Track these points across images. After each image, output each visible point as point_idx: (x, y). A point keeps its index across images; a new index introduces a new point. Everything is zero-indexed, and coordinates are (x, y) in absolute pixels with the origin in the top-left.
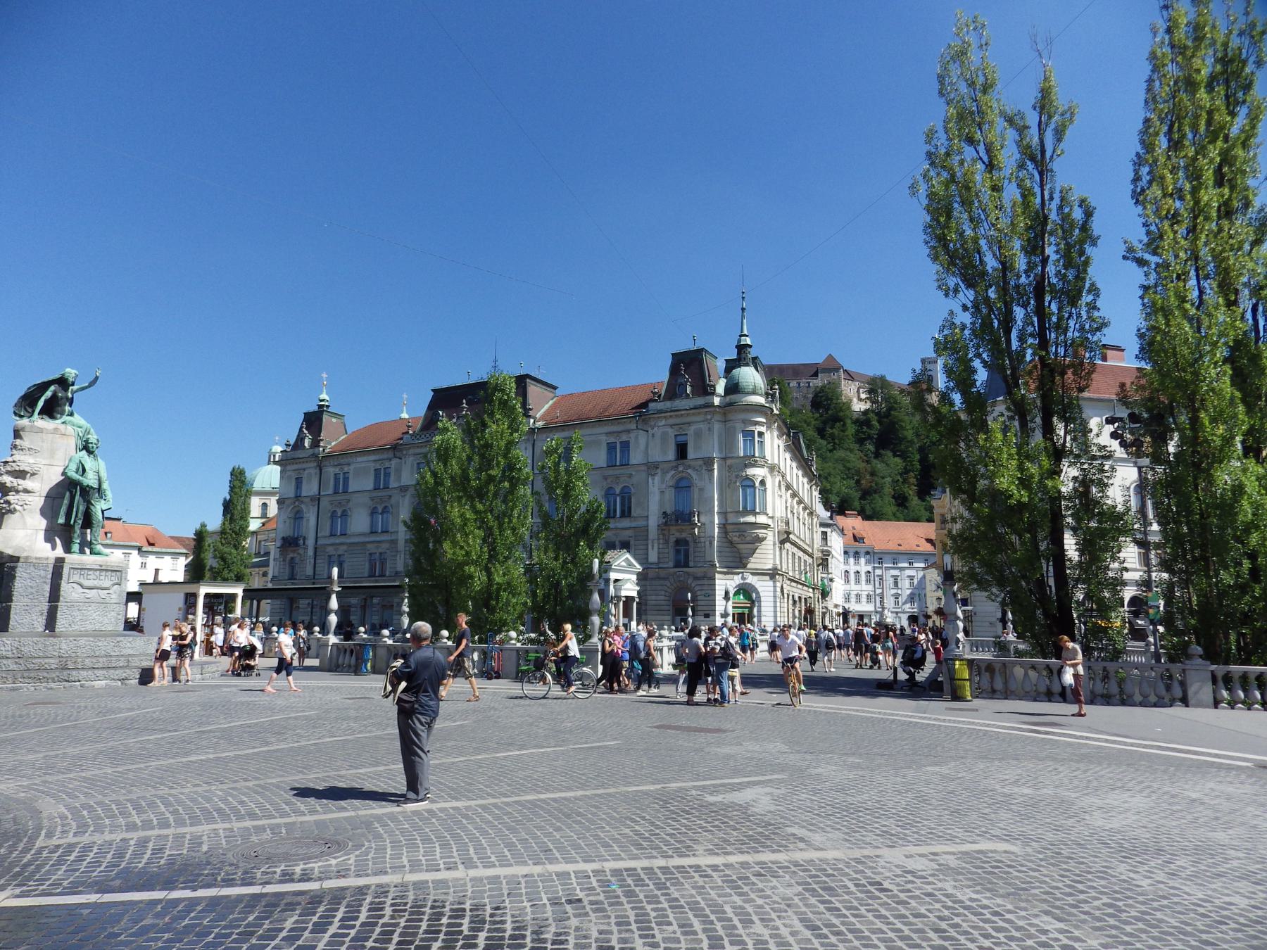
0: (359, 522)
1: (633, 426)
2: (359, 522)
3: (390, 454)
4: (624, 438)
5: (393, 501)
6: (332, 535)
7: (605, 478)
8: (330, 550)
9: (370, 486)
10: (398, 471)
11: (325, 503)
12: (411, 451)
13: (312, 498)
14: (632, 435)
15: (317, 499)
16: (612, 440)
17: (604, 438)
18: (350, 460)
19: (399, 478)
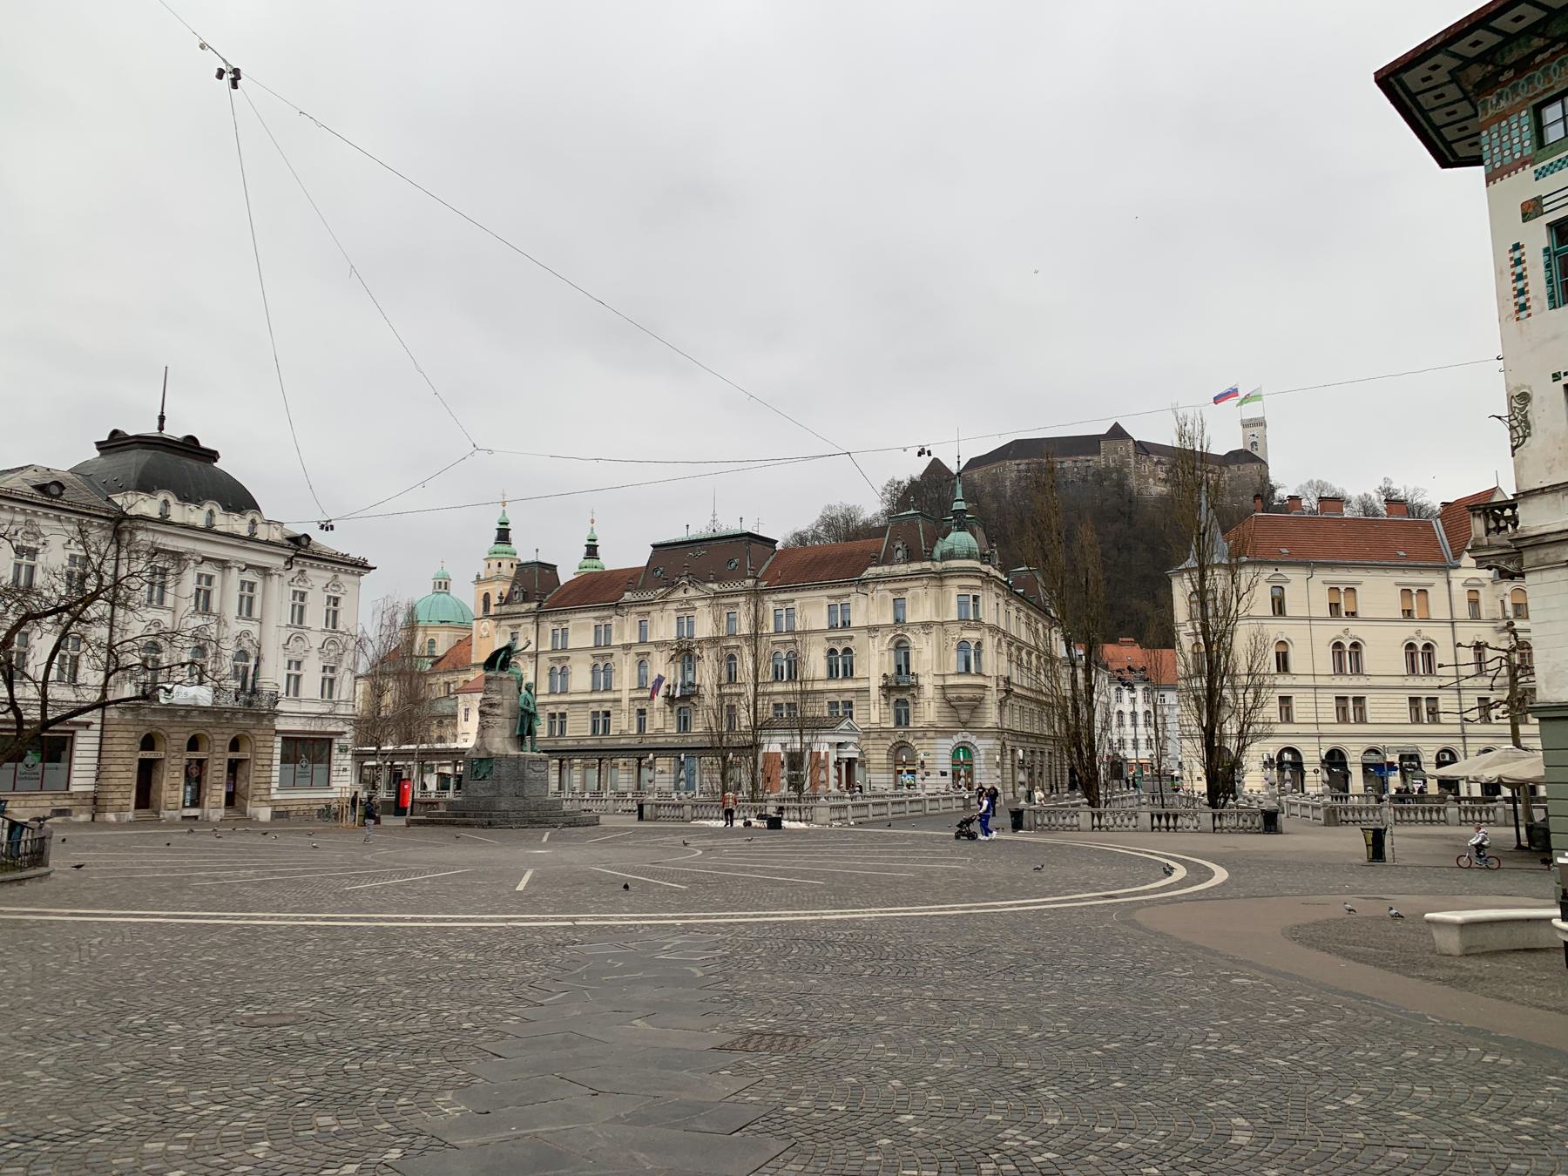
0: (581, 678)
1: (853, 589)
2: (581, 678)
3: (611, 612)
4: (845, 601)
5: (614, 659)
6: (552, 693)
7: (828, 639)
8: (551, 709)
9: (592, 644)
10: (621, 629)
11: (543, 659)
12: (633, 610)
13: (530, 655)
14: (853, 598)
15: (536, 655)
16: (833, 602)
17: (826, 601)
18: (569, 617)
19: (621, 636)
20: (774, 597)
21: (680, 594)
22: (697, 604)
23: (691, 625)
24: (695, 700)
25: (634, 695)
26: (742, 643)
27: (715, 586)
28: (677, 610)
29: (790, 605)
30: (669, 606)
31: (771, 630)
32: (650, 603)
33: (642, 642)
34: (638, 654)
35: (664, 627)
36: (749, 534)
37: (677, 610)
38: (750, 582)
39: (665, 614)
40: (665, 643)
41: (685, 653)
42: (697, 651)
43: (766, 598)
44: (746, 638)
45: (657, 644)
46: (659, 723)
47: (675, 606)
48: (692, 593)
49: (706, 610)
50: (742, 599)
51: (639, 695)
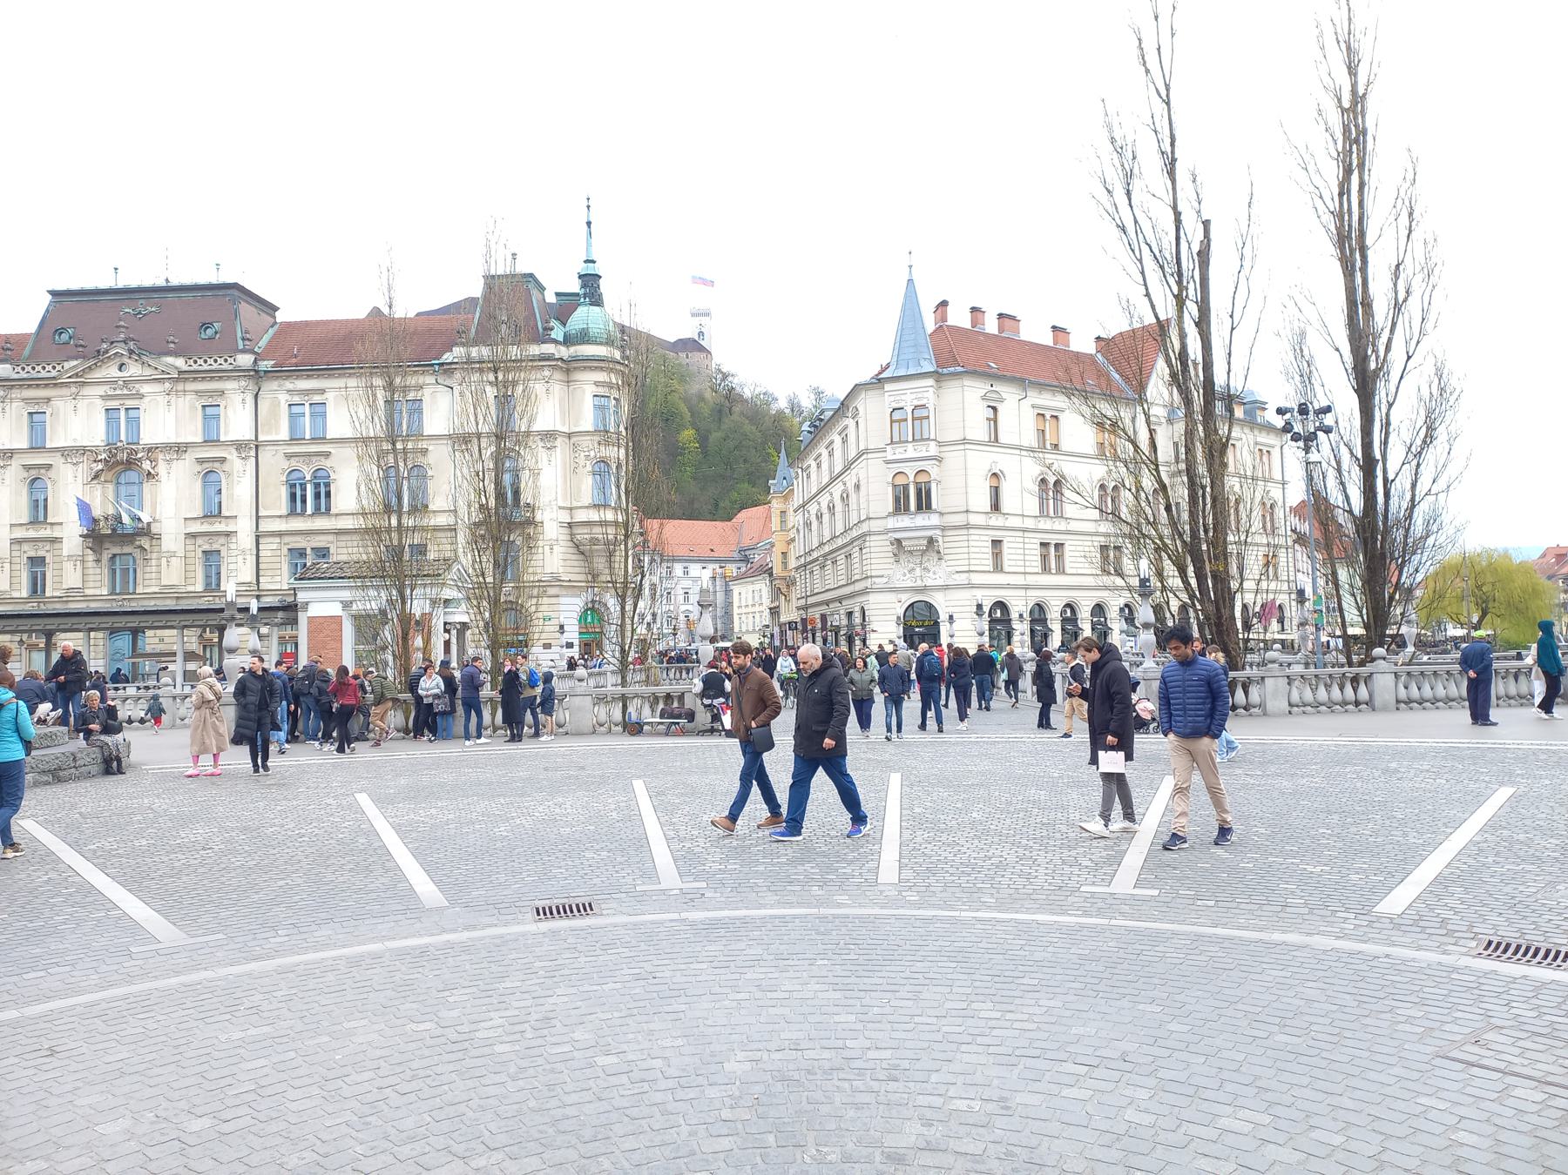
1: (430, 379)
12: (16, 393)
14: (427, 392)
20: (289, 385)
21: (111, 371)
22: (145, 389)
23: (134, 424)
24: (144, 542)
25: (20, 533)
26: (231, 455)
27: (180, 363)
28: (106, 397)
29: (317, 398)
30: (87, 391)
31: (284, 434)
32: (51, 383)
33: (37, 447)
34: (27, 468)
35: (80, 421)
36: (235, 286)
37: (106, 397)
38: (245, 360)
39: (82, 404)
40: (83, 450)
41: (122, 463)
42: (146, 465)
43: (274, 385)
44: (240, 446)
45: (66, 452)
46: (72, 578)
47: (101, 390)
48: (134, 369)
49: (162, 400)
50: (229, 385)
51: (32, 534)
